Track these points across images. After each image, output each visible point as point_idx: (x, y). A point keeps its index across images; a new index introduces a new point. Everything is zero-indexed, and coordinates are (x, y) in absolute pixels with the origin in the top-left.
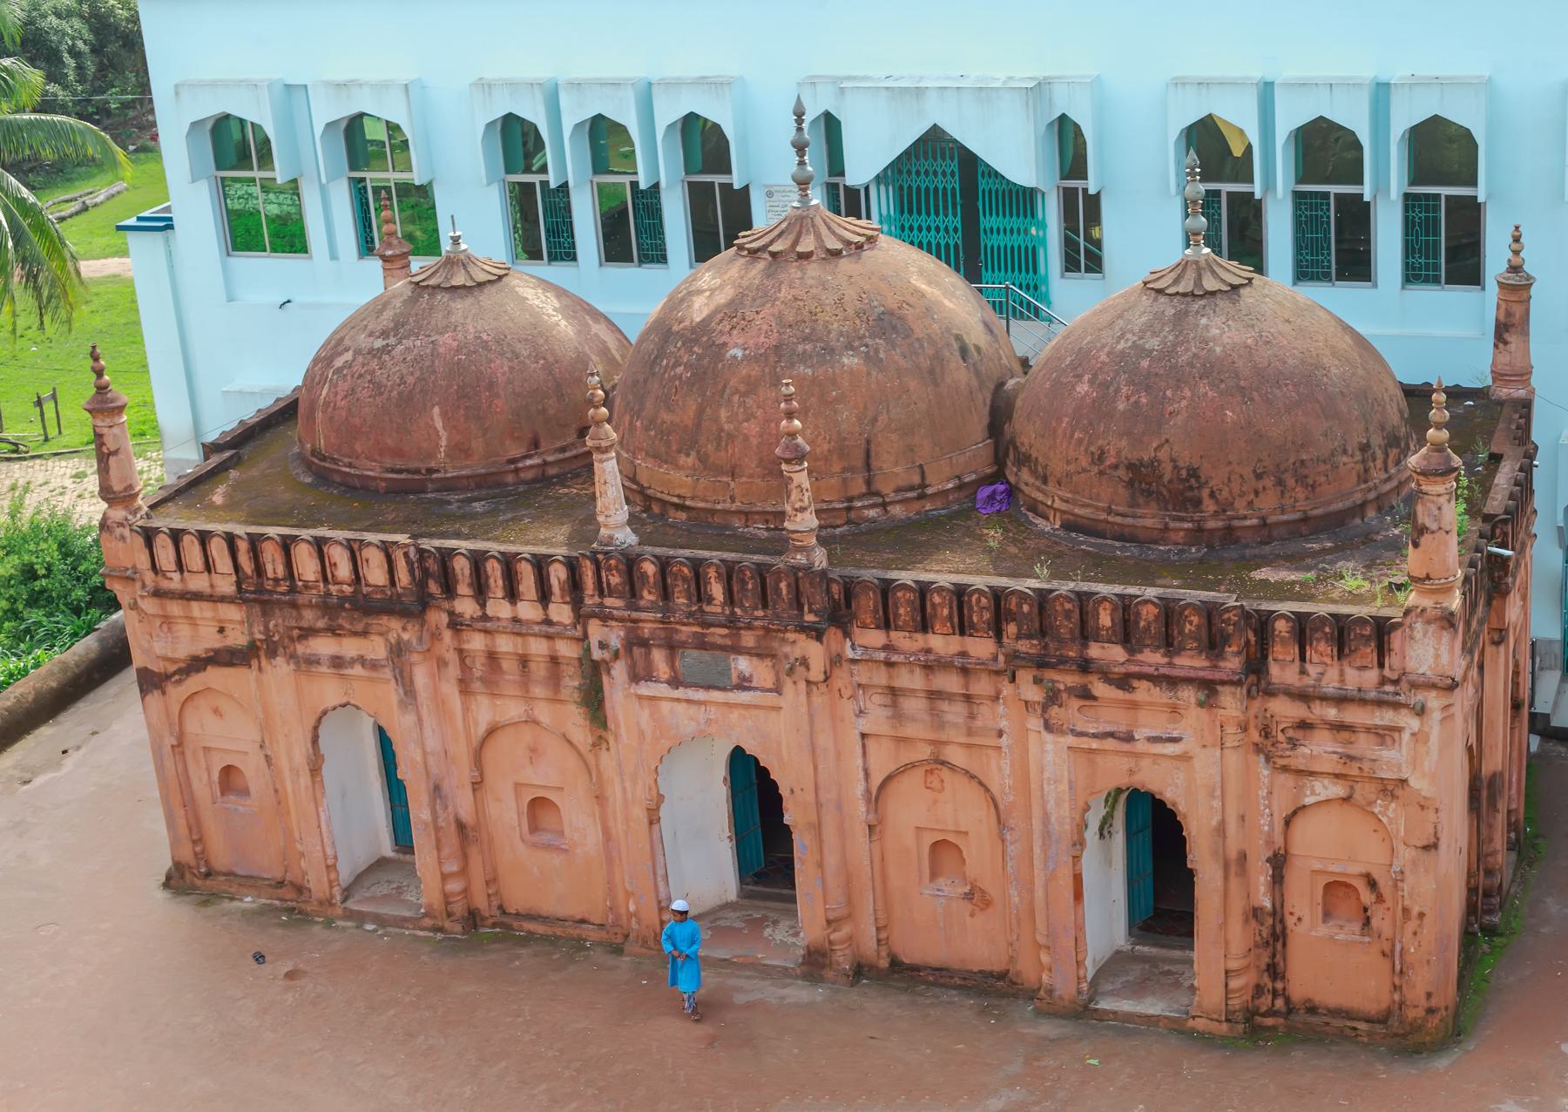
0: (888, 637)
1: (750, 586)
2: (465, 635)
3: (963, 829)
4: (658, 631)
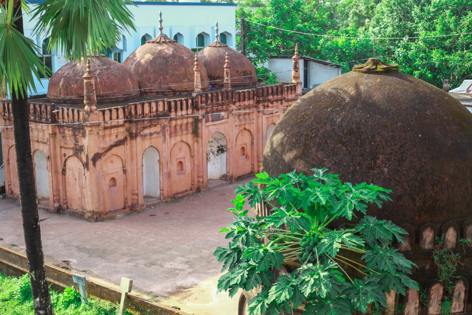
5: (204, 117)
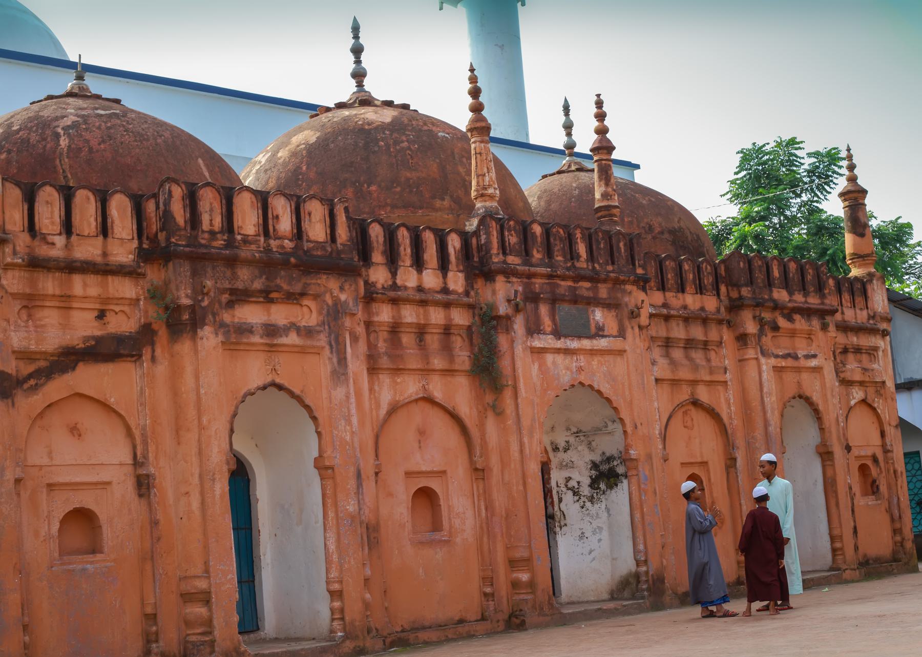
0: (665, 297)
1: (602, 246)
2: (375, 306)
3: (705, 460)
4: (545, 286)
5: (517, 309)
